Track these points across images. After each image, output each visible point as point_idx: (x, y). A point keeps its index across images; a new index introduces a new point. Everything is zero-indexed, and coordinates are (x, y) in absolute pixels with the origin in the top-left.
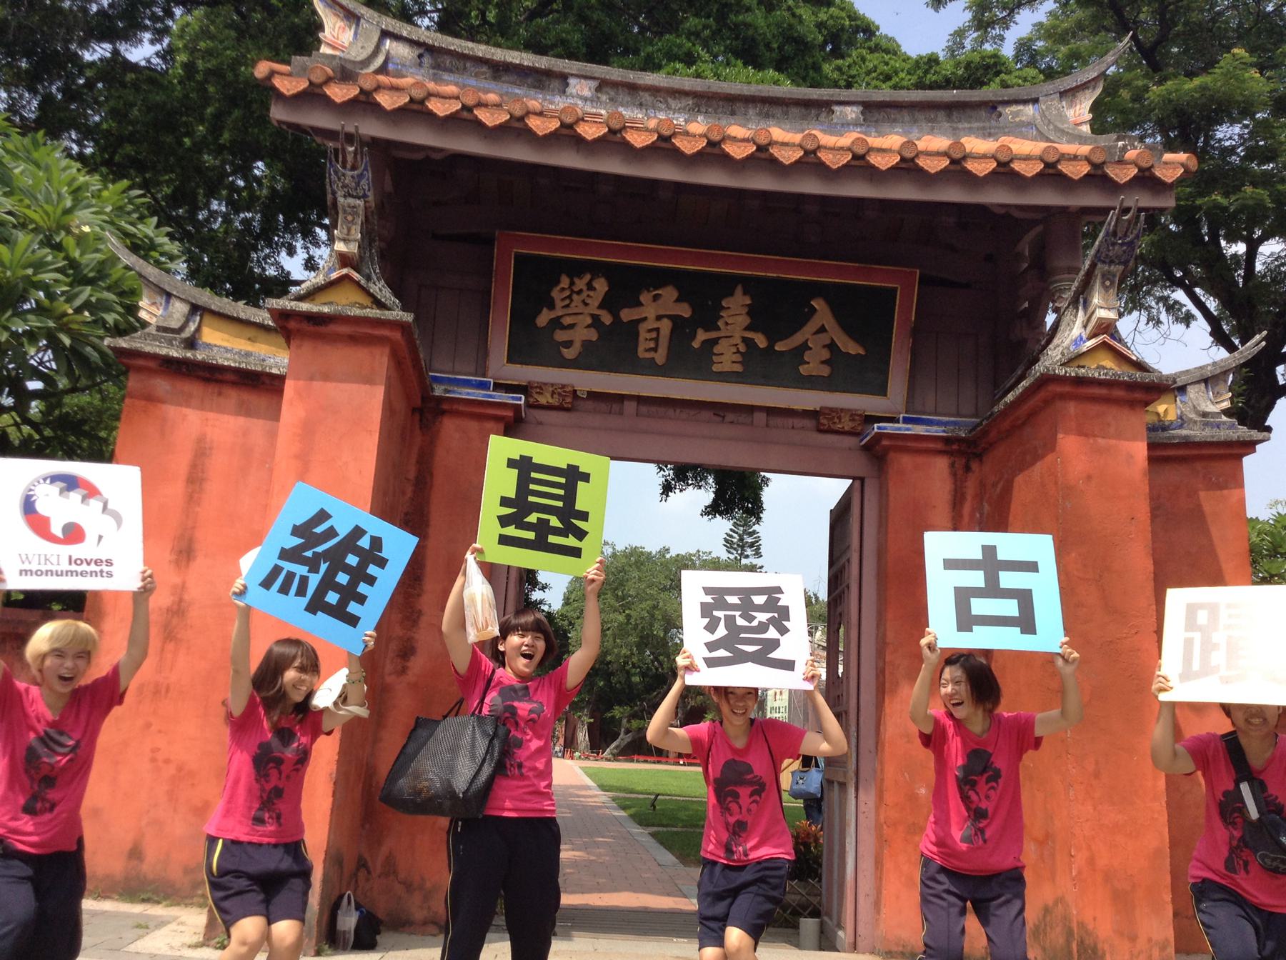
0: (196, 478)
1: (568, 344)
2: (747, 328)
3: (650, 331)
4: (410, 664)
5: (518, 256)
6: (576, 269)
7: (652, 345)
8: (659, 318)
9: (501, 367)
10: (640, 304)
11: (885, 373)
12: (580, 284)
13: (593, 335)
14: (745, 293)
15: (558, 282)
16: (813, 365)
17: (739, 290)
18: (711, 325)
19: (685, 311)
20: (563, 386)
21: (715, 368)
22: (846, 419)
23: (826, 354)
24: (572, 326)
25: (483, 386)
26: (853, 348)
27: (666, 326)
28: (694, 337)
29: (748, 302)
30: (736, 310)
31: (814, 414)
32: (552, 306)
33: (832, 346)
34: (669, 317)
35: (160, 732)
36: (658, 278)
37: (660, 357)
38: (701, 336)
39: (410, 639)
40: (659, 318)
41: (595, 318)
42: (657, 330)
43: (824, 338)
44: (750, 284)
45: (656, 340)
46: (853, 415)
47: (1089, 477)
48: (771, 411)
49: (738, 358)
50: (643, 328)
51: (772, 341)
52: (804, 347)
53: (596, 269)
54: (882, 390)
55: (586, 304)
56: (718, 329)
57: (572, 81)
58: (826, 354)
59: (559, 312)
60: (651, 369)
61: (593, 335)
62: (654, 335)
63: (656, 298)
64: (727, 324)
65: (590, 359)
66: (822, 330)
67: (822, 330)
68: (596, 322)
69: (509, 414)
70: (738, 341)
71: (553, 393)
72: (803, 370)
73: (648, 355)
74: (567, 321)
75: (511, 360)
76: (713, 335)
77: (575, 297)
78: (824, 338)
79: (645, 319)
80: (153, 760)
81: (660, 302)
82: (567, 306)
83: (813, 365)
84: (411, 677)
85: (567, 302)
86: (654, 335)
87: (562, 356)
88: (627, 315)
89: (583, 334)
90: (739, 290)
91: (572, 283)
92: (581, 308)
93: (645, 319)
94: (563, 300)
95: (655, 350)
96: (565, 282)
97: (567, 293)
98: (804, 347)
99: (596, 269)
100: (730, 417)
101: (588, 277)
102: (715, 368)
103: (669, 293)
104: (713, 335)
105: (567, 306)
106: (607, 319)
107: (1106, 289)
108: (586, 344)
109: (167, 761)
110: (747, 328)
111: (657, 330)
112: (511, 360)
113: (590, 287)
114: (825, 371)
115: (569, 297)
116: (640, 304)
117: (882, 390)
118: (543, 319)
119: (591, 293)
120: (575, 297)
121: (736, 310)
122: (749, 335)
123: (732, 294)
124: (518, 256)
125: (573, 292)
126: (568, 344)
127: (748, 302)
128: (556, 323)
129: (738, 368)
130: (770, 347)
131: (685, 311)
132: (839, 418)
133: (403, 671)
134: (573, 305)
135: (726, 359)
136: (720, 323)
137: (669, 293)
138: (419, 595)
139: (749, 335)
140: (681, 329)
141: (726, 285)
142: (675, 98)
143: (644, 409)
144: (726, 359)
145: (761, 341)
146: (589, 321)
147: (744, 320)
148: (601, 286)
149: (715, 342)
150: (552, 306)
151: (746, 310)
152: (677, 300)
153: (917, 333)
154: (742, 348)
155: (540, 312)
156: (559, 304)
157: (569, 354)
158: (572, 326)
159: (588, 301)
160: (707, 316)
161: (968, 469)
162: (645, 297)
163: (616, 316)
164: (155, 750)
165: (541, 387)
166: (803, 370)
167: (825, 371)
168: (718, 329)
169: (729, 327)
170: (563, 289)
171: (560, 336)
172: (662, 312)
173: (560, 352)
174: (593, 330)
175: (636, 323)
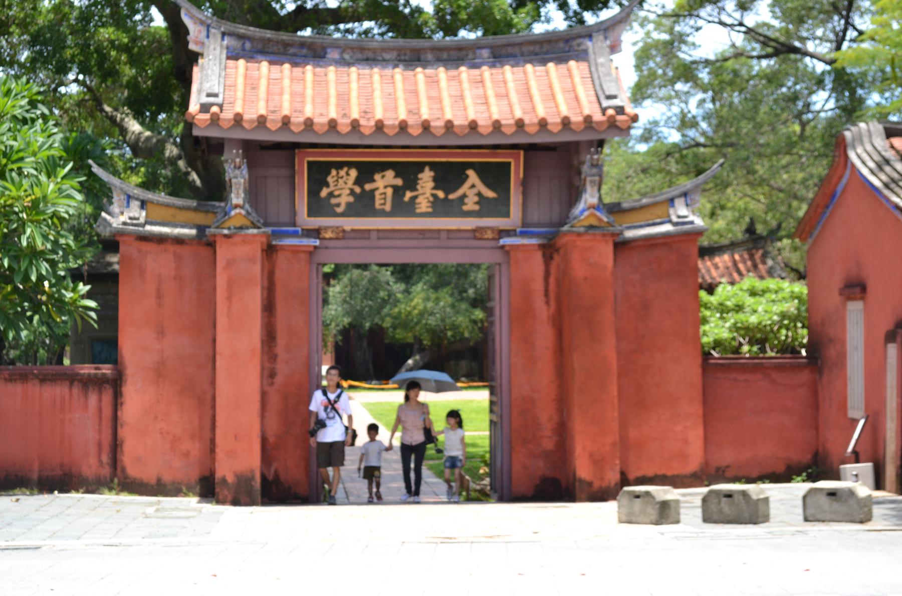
0: (159, 296)
1: (338, 205)
2: (435, 188)
3: (381, 194)
4: (274, 380)
5: (309, 163)
6: (339, 166)
7: (382, 201)
8: (386, 187)
9: (305, 220)
10: (373, 181)
11: (508, 206)
12: (342, 173)
13: (351, 199)
14: (431, 170)
15: (329, 173)
16: (471, 204)
17: (427, 169)
18: (413, 188)
19: (399, 182)
20: (337, 227)
21: (418, 211)
22: (489, 232)
23: (476, 199)
24: (339, 196)
25: (295, 234)
26: (490, 194)
27: (390, 191)
28: (404, 195)
29: (432, 174)
30: (426, 178)
31: (474, 231)
32: (328, 185)
33: (479, 194)
35: (162, 420)
36: (383, 167)
37: (388, 207)
38: (409, 195)
39: (274, 368)
40: (386, 187)
42: (385, 193)
43: (475, 191)
44: (433, 166)
45: (385, 199)
46: (492, 229)
47: (586, 278)
48: (449, 231)
49: (429, 204)
50: (377, 193)
51: (447, 192)
52: (464, 196)
53: (350, 165)
54: (507, 215)
56: (416, 190)
57: (329, 50)
58: (476, 199)
59: (332, 188)
60: (383, 214)
61: (351, 199)
62: (383, 196)
63: (383, 177)
64: (422, 187)
65: (351, 211)
66: (473, 186)
67: (473, 186)
68: (352, 192)
69: (312, 249)
70: (428, 195)
71: (332, 232)
72: (465, 208)
73: (382, 207)
74: (336, 193)
75: (309, 215)
76: (415, 193)
77: (340, 180)
78: (475, 191)
79: (377, 189)
80: (161, 433)
81: (385, 178)
82: (336, 185)
83: (471, 204)
84: (276, 387)
85: (336, 183)
86: (383, 196)
87: (335, 212)
88: (368, 187)
89: (345, 199)
90: (427, 169)
91: (338, 173)
92: (344, 185)
93: (377, 189)
94: (334, 182)
95: (384, 204)
96: (334, 172)
97: (335, 178)
98: (464, 196)
99: (350, 165)
100: (428, 235)
101: (346, 169)
102: (418, 211)
103: (390, 174)
104: (415, 193)
105: (336, 185)
106: (358, 190)
107: (592, 187)
108: (348, 205)
109: (168, 433)
111: (385, 193)
112: (309, 215)
113: (348, 174)
114: (477, 207)
115: (337, 181)
116: (373, 181)
117: (507, 215)
118: (324, 193)
119: (348, 177)
120: (340, 180)
121: (426, 178)
123: (422, 171)
124: (309, 163)
125: (338, 178)
126: (338, 205)
127: (432, 174)
128: (331, 195)
129: (430, 210)
130: (446, 198)
131: (399, 182)
132: (486, 232)
133: (272, 384)
134: (339, 184)
135: (423, 205)
136: (418, 187)
137: (390, 174)
138: (275, 346)
140: (398, 191)
141: (420, 167)
142: (386, 52)
143: (381, 235)
144: (423, 205)
145: (441, 194)
146: (348, 192)
147: (431, 184)
148: (354, 173)
149: (416, 197)
150: (328, 185)
151: (431, 179)
152: (396, 176)
153: (525, 184)
154: (431, 199)
155: (321, 190)
156: (332, 184)
157: (339, 210)
158: (339, 196)
159: (347, 181)
160: (411, 183)
161: (551, 258)
162: (377, 177)
163: (362, 187)
164: (161, 429)
165: (326, 228)
166: (465, 208)
167: (477, 207)
168: (416, 190)
170: (333, 177)
171: (334, 201)
172: (387, 184)
175: (373, 191)
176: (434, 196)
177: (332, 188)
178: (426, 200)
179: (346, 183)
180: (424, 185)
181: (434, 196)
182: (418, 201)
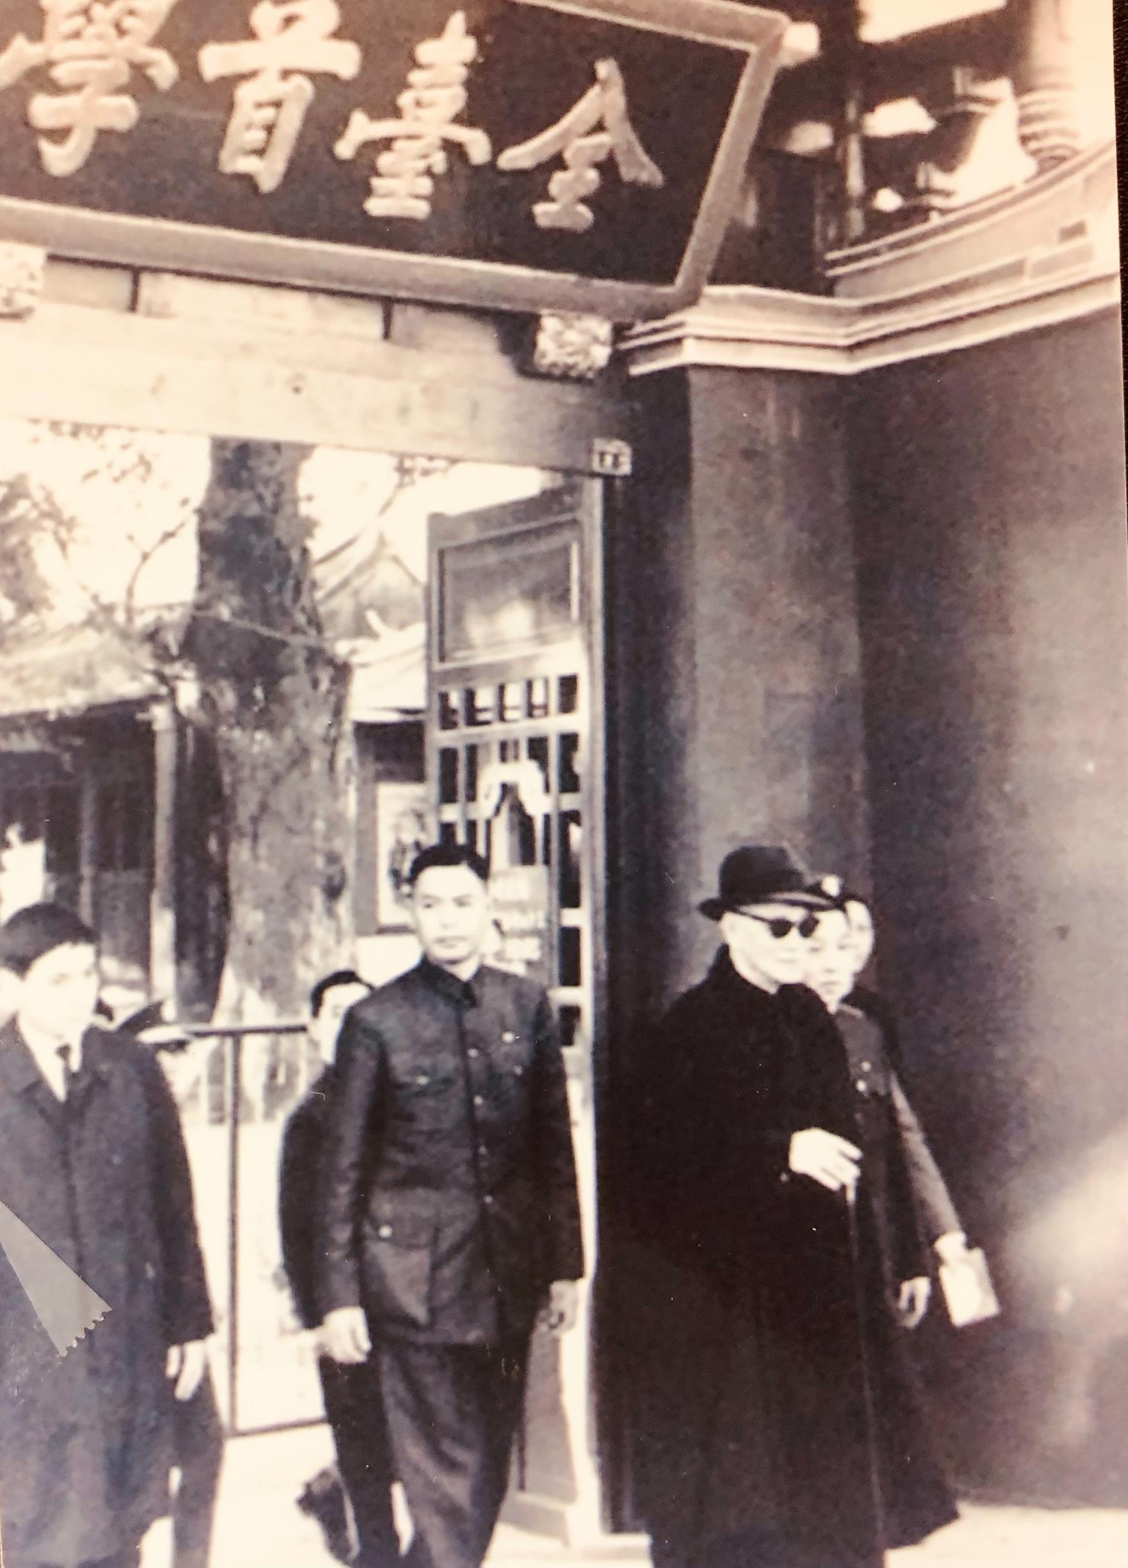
1: (59, 135)
2: (458, 120)
32: (36, 35)
34: (312, 76)
41: (138, 69)
51: (498, 148)
55: (121, 31)
56: (396, 113)
79: (252, 75)
82: (76, 35)
105: (76, 35)
110: (458, 120)
122: (461, 134)
126: (59, 135)
136: (405, 99)
139: (461, 134)
147: (454, 98)
149: (386, 144)
150: (36, 35)
154: (439, 162)
159: (128, 22)
169: (421, 112)
172: (290, 64)
173: (37, 155)
174: (126, 101)
175: (229, 83)
176: (454, 150)
177: (53, 47)
178: (422, 165)
179: (121, 31)
180: (427, 96)
181: (454, 150)
182: (384, 161)
